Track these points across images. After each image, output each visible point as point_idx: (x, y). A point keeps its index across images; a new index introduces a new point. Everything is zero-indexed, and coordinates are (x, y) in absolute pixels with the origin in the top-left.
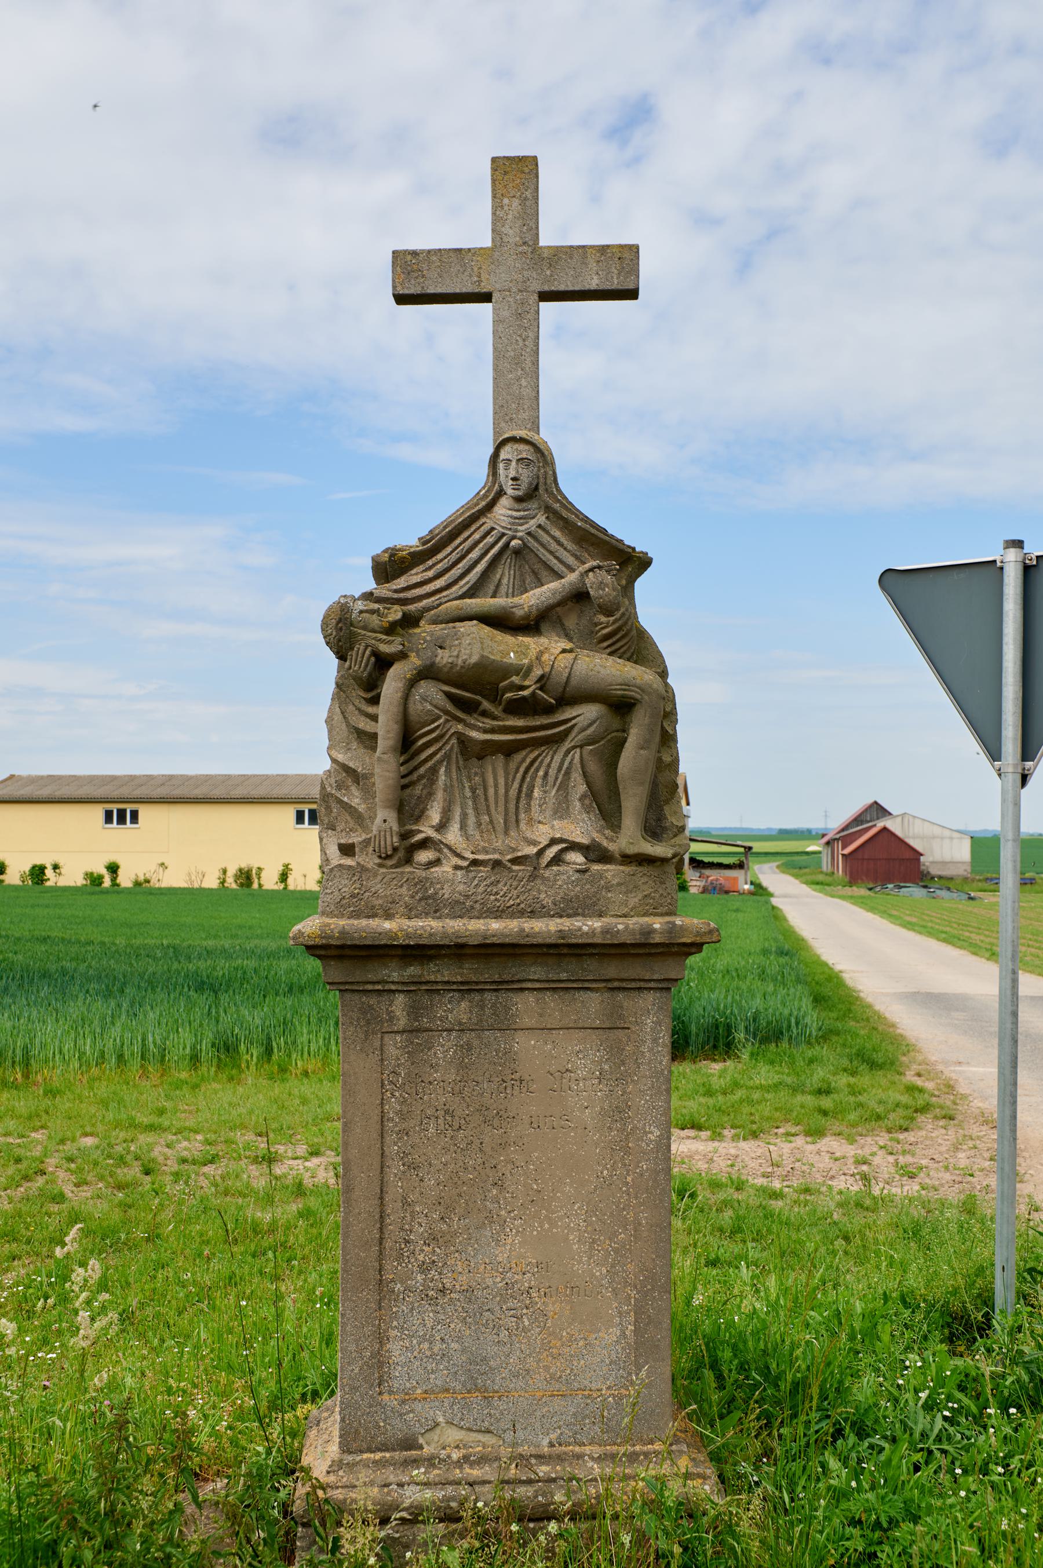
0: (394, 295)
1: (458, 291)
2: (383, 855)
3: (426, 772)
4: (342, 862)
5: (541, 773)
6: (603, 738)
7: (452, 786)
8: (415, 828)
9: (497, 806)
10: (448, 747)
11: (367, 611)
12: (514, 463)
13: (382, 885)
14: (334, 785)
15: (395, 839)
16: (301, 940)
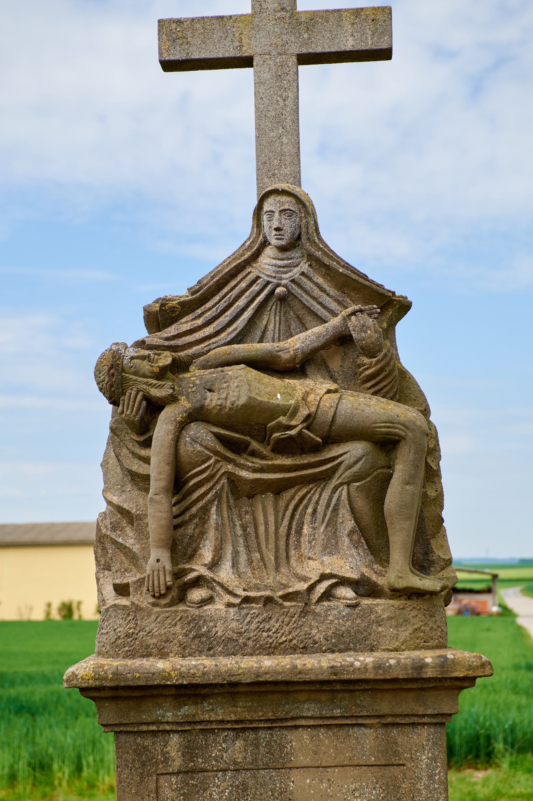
0: (161, 62)
1: (221, 56)
2: (157, 595)
3: (198, 511)
4: (117, 602)
5: (310, 510)
6: (369, 475)
7: (223, 525)
8: (187, 566)
9: (267, 544)
10: (218, 487)
11: (137, 358)
12: (277, 215)
13: (157, 623)
14: (110, 526)
15: (168, 578)
16: (75, 682)
